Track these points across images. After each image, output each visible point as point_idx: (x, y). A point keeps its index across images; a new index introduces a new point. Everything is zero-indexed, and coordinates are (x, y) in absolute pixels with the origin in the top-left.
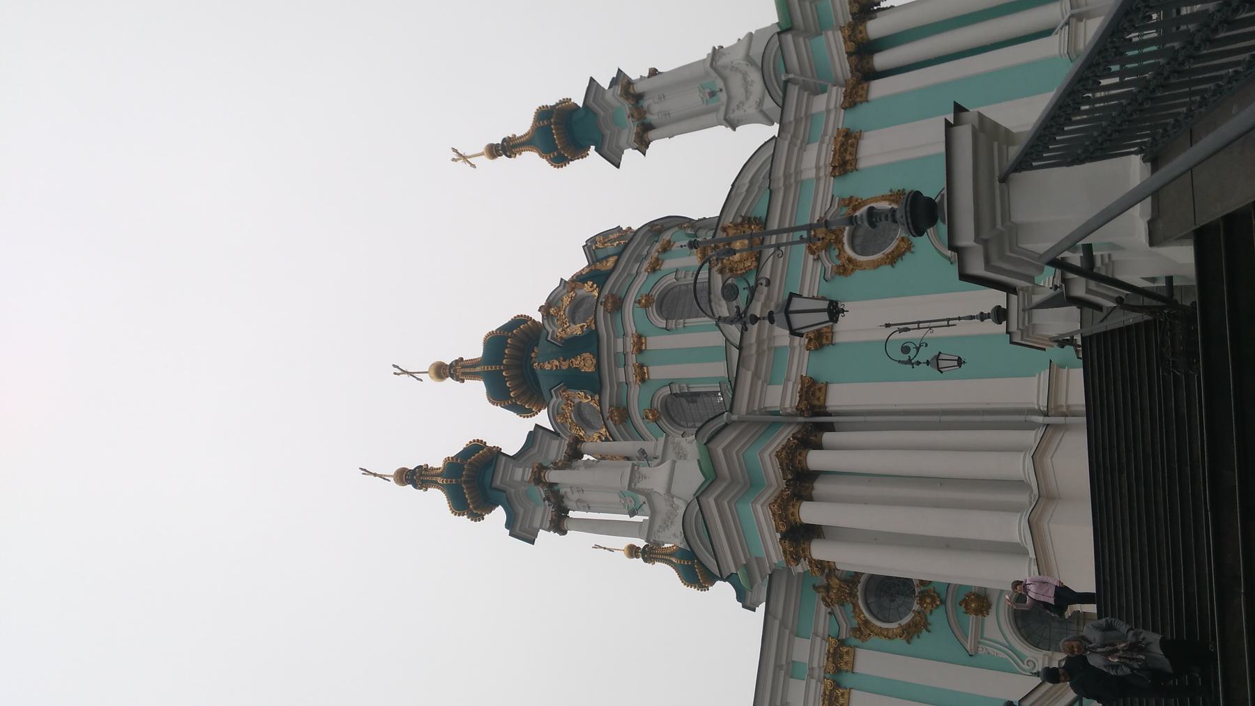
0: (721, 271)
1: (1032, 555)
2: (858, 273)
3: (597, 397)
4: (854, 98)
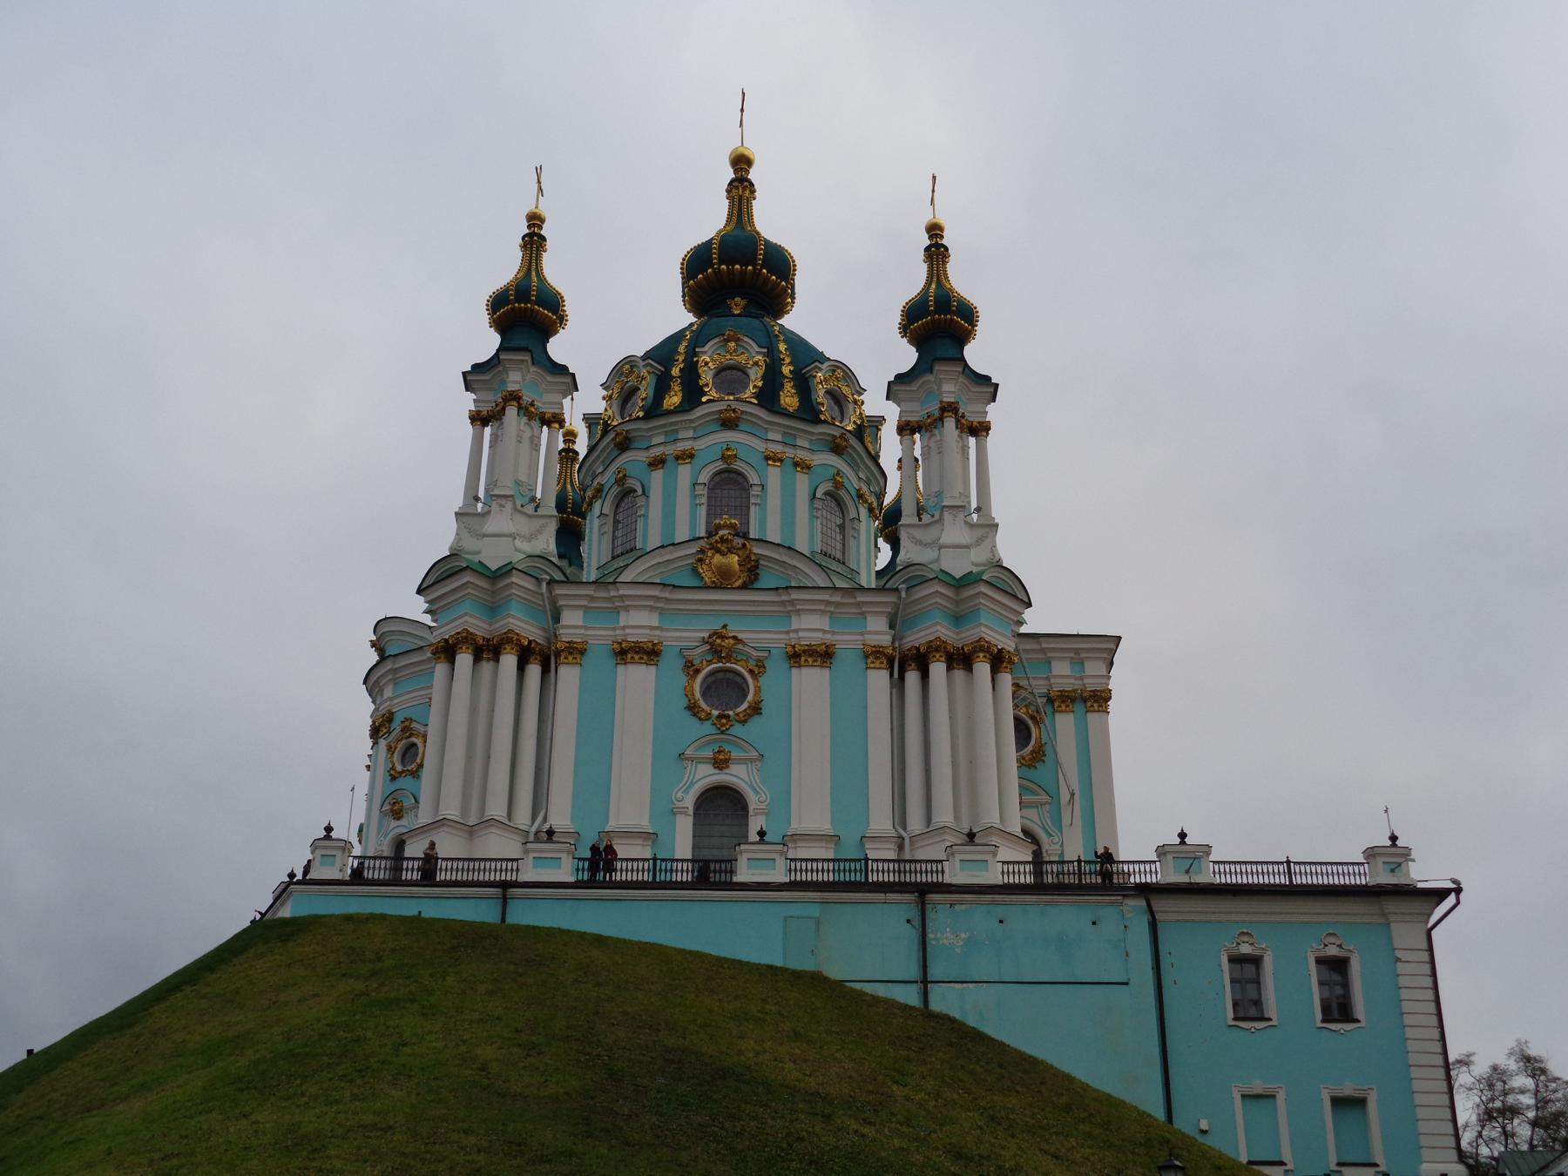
0: (702, 551)
2: (682, 679)
3: (641, 414)
4: (873, 655)
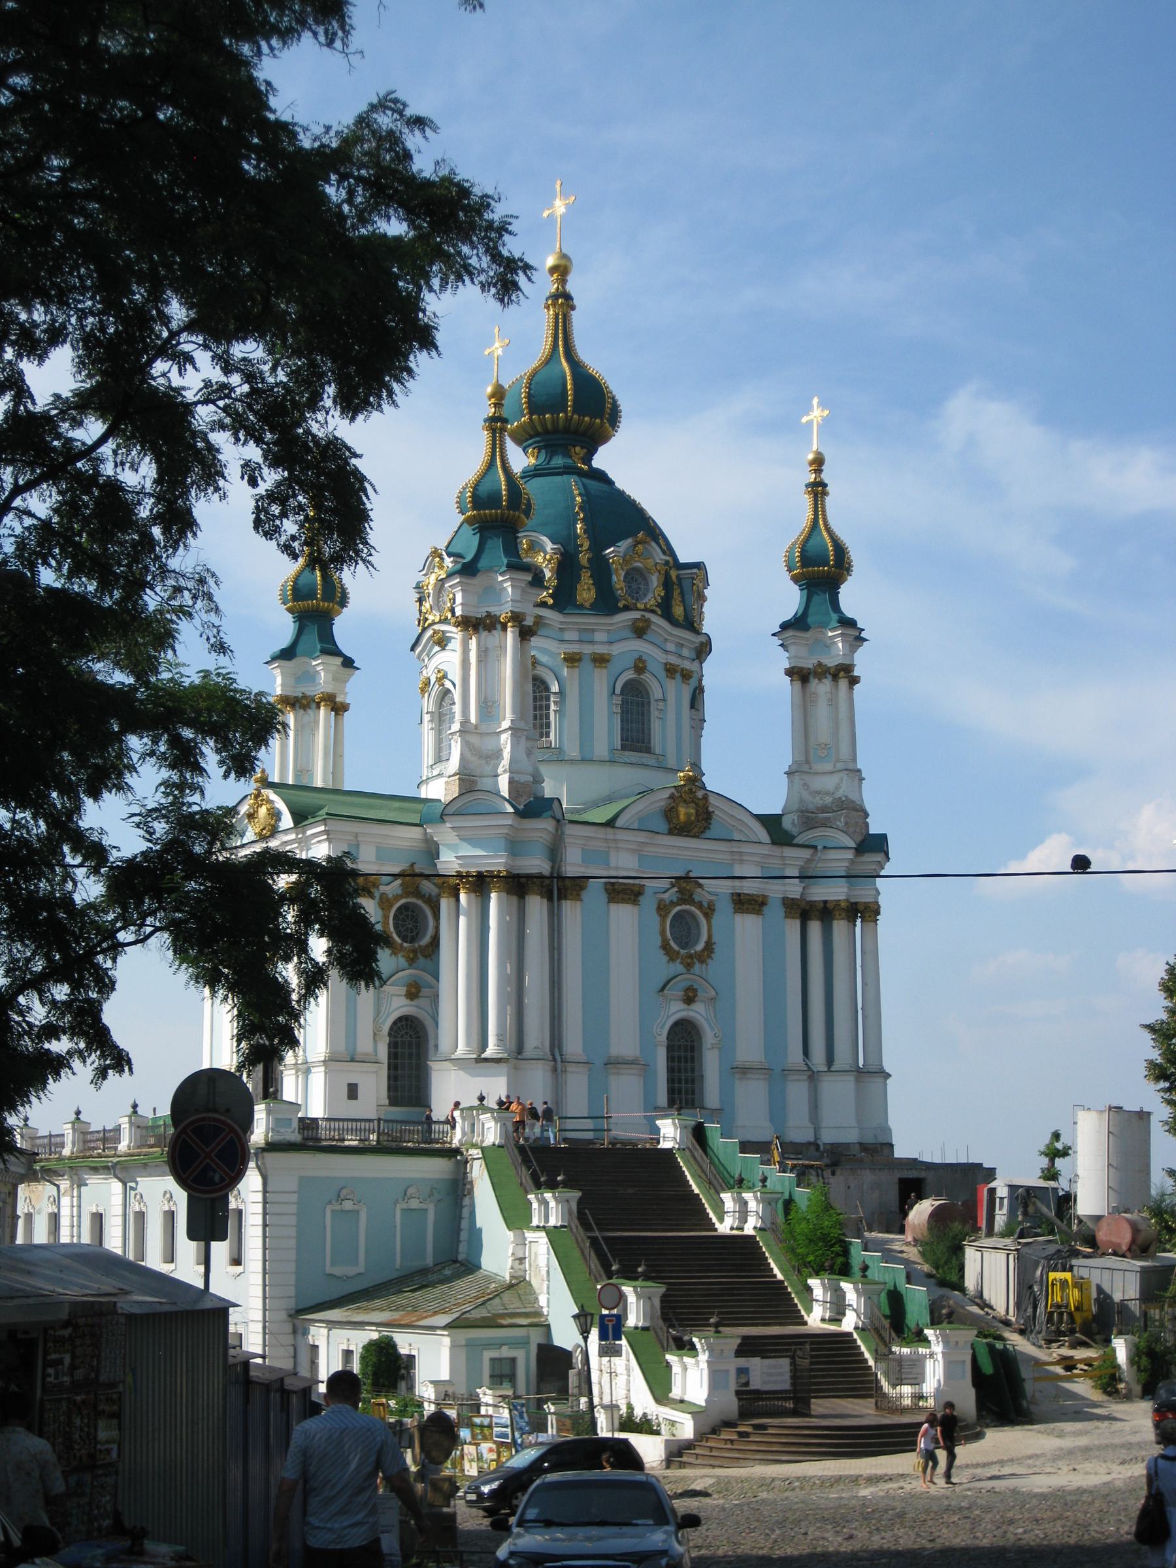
0: (672, 797)
1: (483, 1056)
2: (657, 918)
3: (551, 601)
